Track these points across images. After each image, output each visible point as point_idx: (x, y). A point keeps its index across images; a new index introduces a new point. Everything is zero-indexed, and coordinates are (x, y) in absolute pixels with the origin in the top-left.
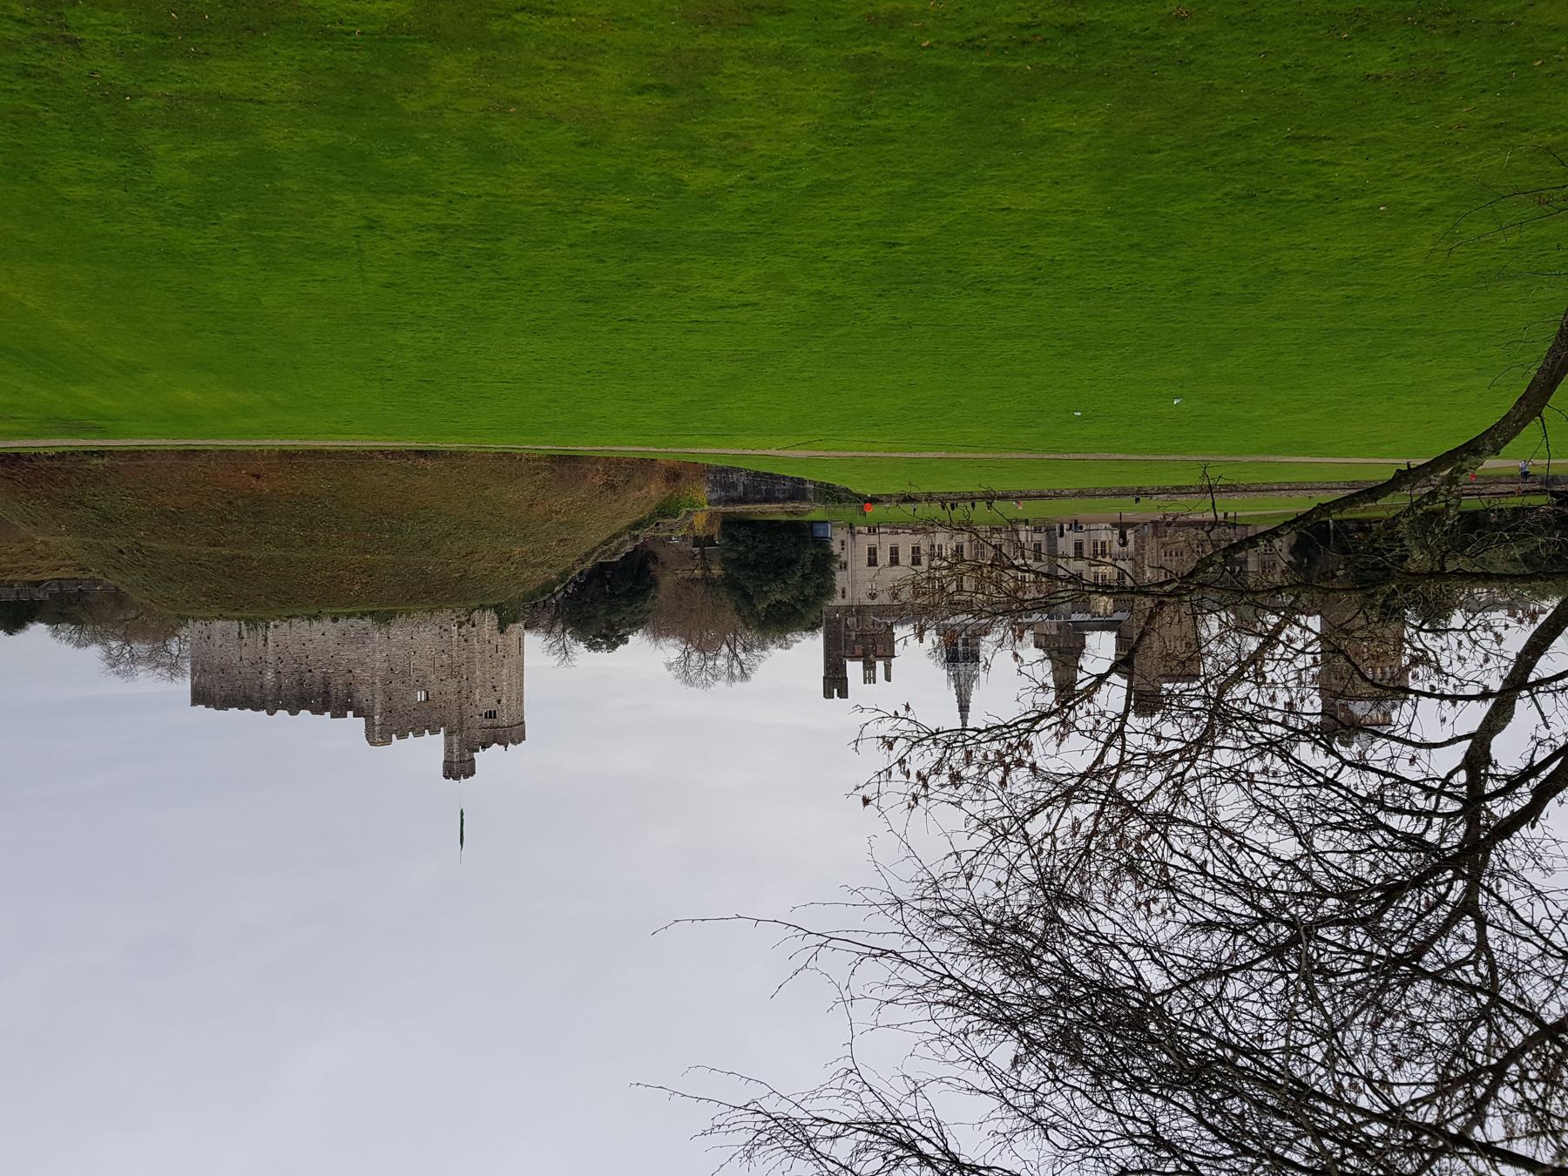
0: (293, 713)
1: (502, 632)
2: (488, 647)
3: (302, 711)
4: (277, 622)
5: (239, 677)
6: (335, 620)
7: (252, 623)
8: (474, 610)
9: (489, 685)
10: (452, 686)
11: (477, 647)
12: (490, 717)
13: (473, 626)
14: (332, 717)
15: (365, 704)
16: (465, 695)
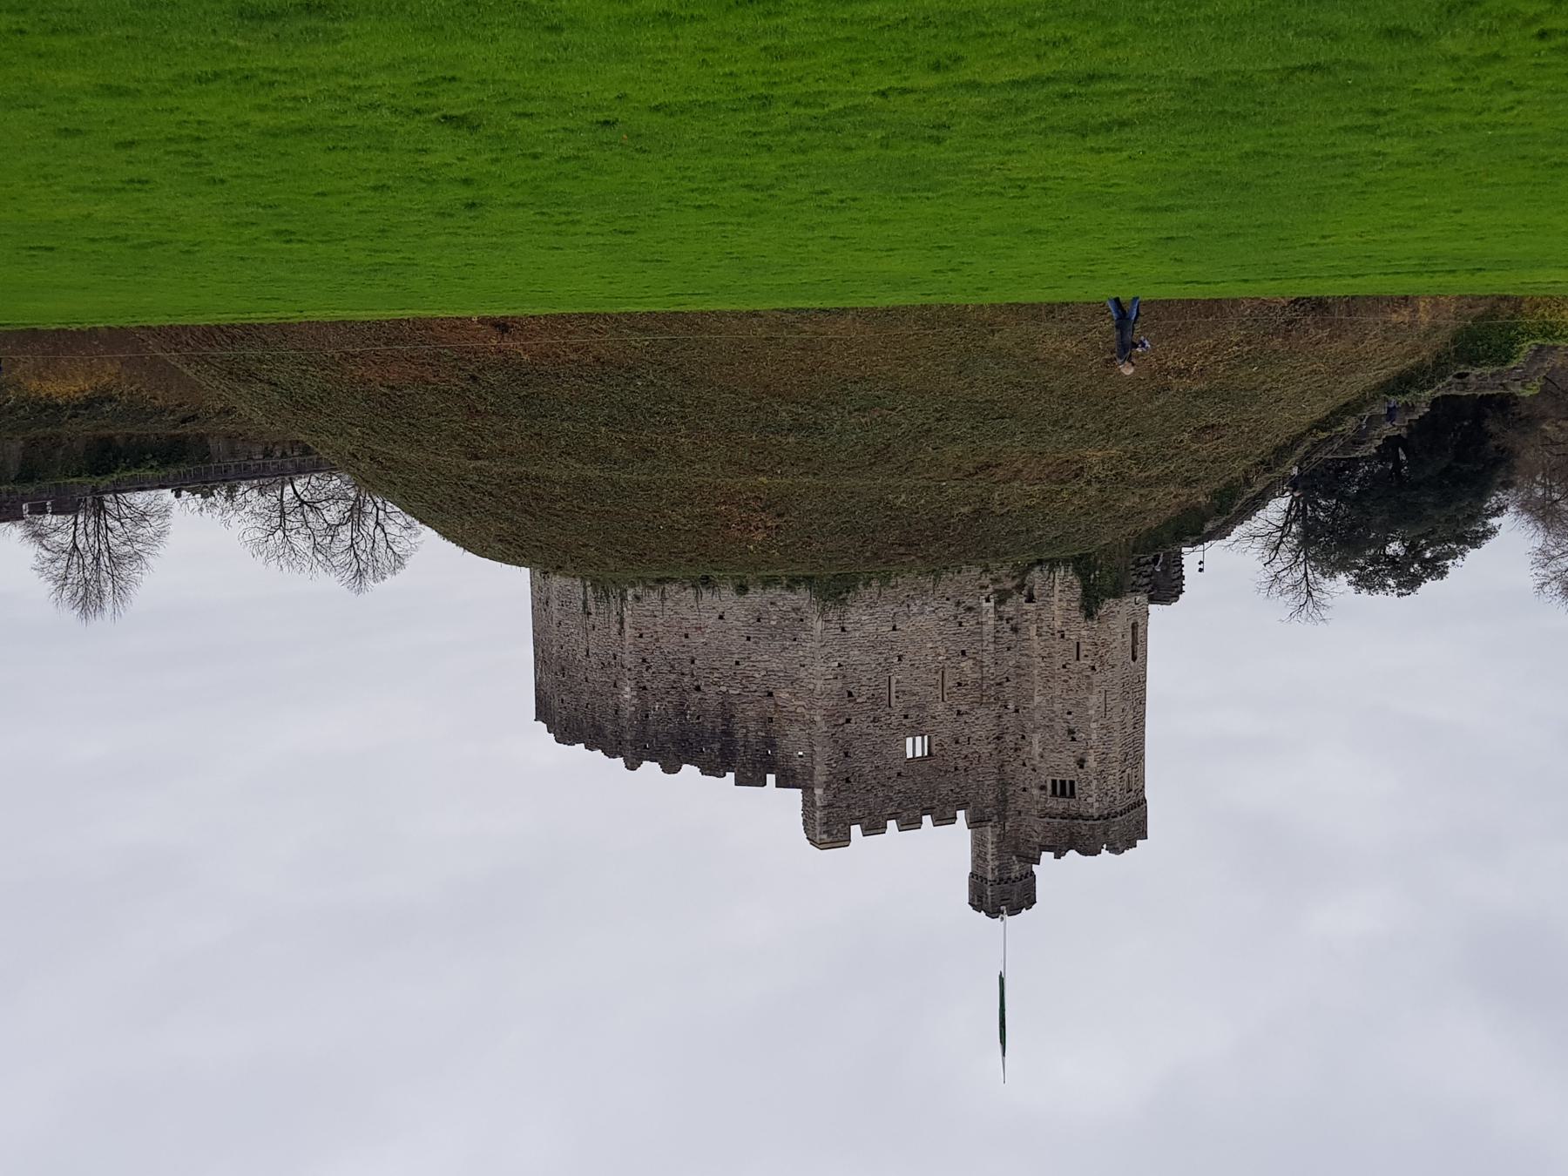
0: (670, 768)
1: (1089, 615)
2: (1059, 646)
3: (685, 767)
4: (639, 590)
5: (584, 686)
6: (742, 589)
7: (603, 588)
8: (1031, 566)
9: (1060, 726)
10: (982, 724)
11: (1036, 644)
12: (1063, 794)
13: (1030, 599)
14: (738, 783)
15: (796, 764)
16: (1008, 743)
